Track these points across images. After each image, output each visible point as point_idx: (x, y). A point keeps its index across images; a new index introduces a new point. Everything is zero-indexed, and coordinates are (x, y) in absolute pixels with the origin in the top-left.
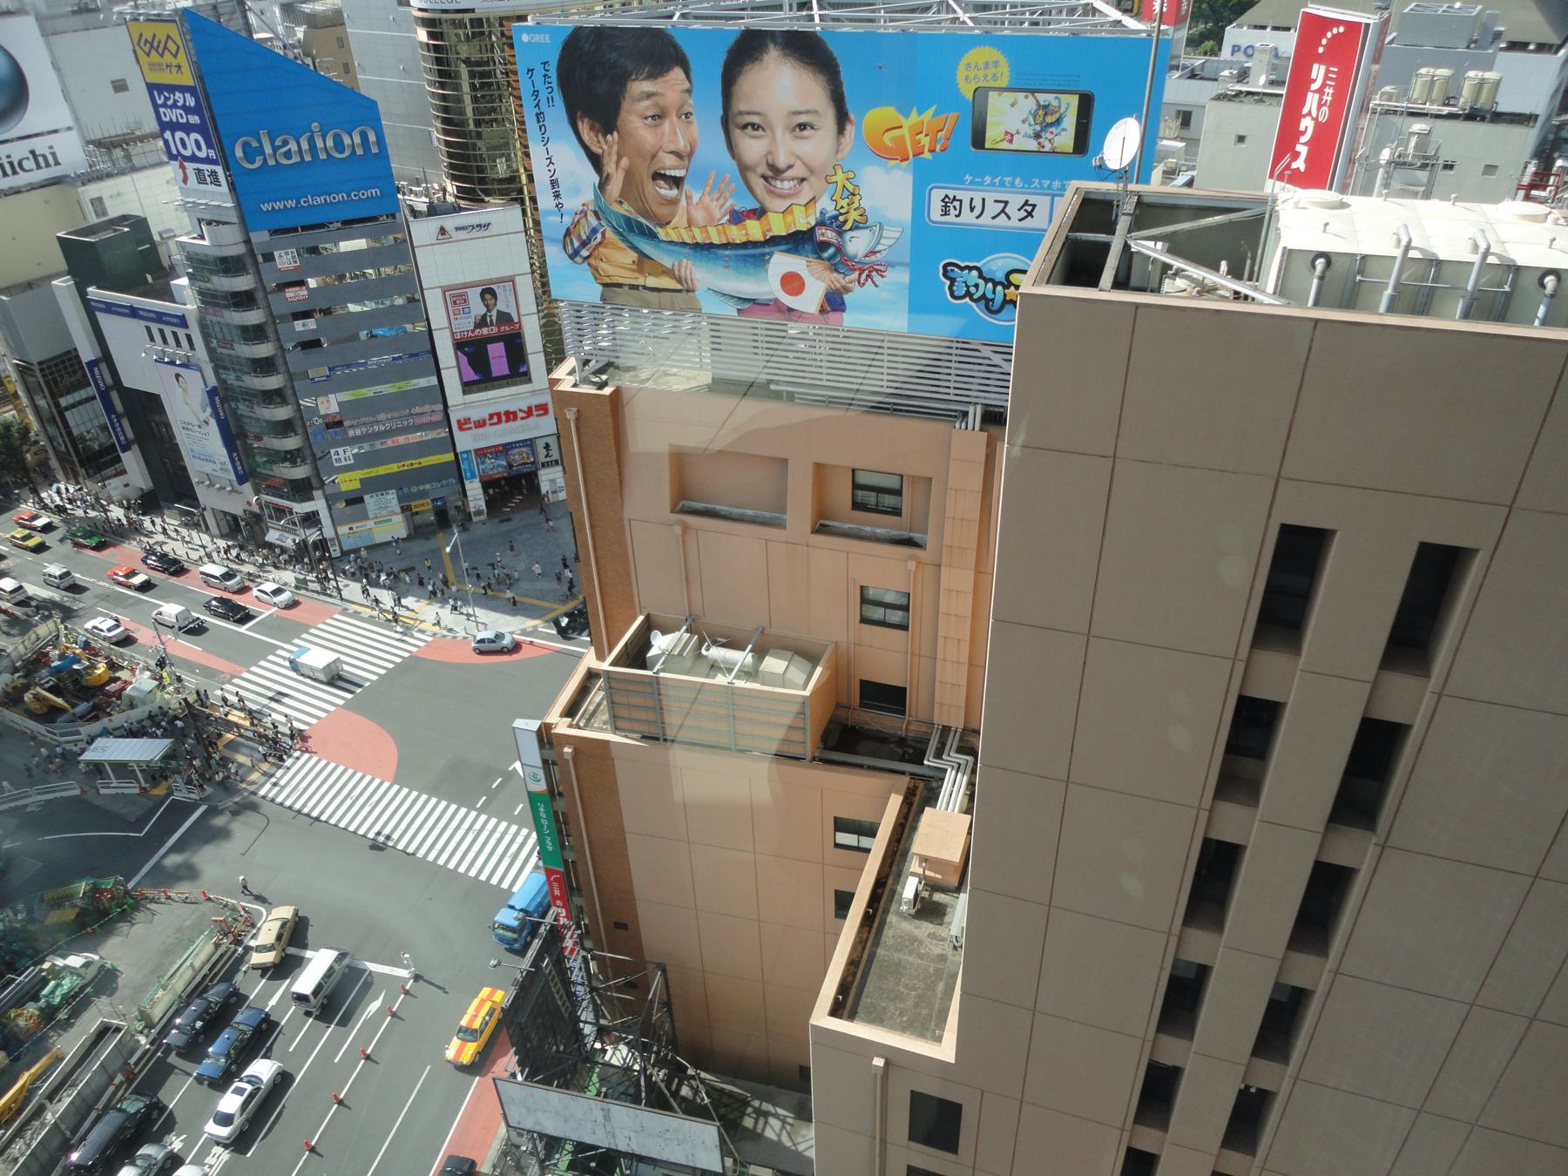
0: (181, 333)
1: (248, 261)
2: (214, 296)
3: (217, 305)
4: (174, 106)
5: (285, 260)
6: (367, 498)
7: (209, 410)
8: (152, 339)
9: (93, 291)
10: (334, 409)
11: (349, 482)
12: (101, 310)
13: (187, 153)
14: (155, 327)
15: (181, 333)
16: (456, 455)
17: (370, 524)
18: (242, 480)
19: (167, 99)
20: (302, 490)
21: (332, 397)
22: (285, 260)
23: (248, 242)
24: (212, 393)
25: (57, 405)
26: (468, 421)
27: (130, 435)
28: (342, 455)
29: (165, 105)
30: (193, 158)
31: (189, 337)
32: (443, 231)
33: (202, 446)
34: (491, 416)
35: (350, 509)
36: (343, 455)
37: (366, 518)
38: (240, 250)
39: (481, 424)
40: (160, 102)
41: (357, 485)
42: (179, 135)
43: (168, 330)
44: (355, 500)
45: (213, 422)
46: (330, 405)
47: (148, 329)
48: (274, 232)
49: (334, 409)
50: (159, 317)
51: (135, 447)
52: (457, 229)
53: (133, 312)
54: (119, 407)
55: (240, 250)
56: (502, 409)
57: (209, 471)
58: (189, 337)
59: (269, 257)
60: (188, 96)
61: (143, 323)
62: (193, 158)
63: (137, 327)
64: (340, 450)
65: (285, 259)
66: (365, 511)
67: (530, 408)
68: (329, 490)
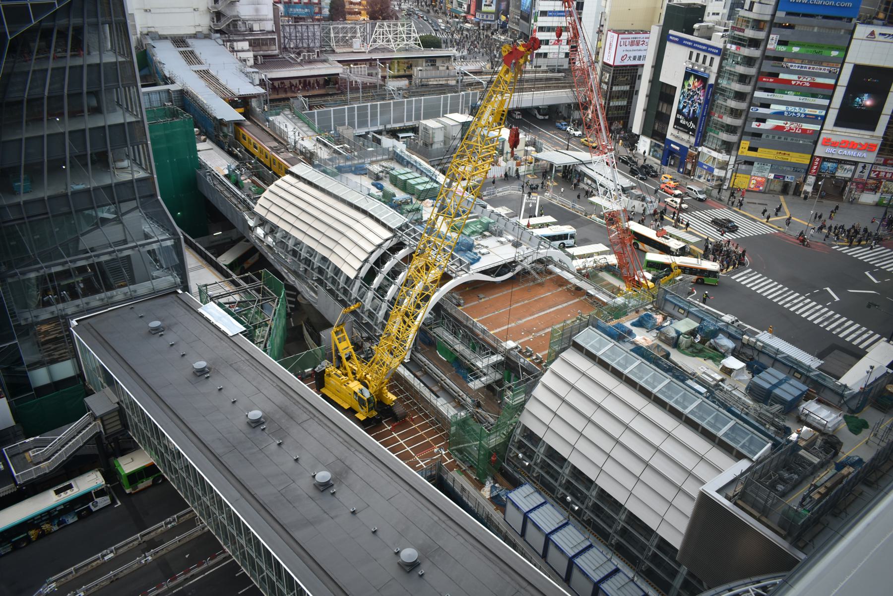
1: (768, 25)
2: (740, 39)
6: (756, 164)
8: (690, 58)
9: (671, 32)
14: (695, 52)
16: (813, 158)
23: (773, 15)
25: (611, 88)
26: (829, 140)
32: (872, 33)
34: (844, 142)
35: (744, 167)
38: (768, 18)
39: (834, 145)
47: (691, 53)
48: (788, 14)
52: (880, 34)
55: (768, 18)
56: (850, 139)
61: (689, 50)
67: (866, 144)
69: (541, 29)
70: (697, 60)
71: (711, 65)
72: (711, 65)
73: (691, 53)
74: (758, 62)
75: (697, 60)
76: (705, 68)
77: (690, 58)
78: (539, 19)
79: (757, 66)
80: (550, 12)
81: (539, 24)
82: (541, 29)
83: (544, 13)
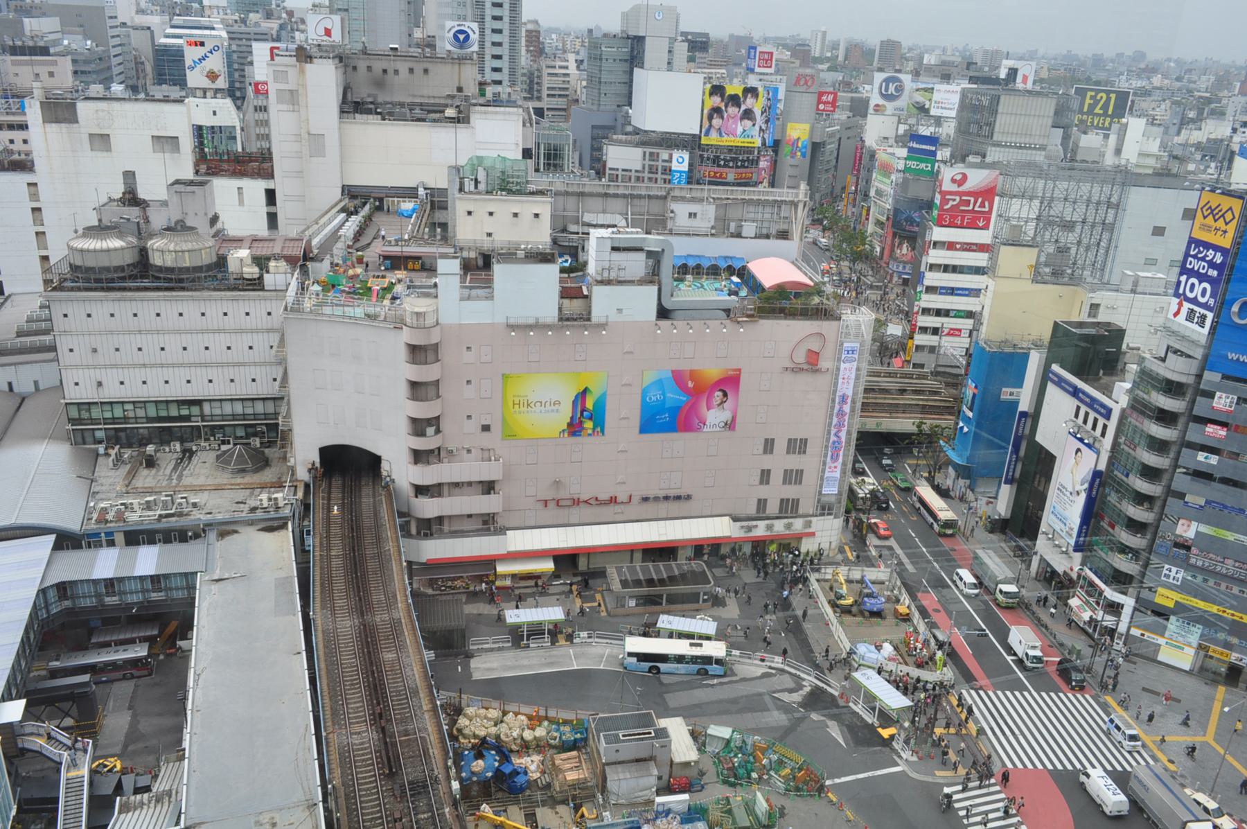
0: (1101, 421)
2: (1145, 406)
3: (1143, 413)
4: (1203, 259)
5: (1223, 402)
6: (1173, 618)
7: (1086, 486)
8: (1077, 416)
9: (1055, 368)
10: (1190, 534)
11: (1165, 597)
12: (1053, 381)
13: (1191, 296)
14: (1083, 409)
15: (1101, 421)
17: (1161, 641)
18: (1077, 548)
19: (1200, 252)
20: (1120, 580)
21: (1194, 525)
22: (1223, 402)
23: (1199, 377)
24: (1096, 474)
27: (1017, 475)
28: (1173, 574)
29: (1195, 257)
30: (1194, 301)
31: (1105, 427)
33: (1064, 508)
36: (1175, 574)
37: (1162, 635)
38: (1190, 380)
40: (1192, 253)
41: (1171, 605)
42: (1194, 280)
43: (1092, 415)
44: (1162, 613)
45: (1083, 496)
46: (1188, 530)
47: (1078, 408)
48: (1225, 377)
49: (1190, 534)
50: (1092, 403)
51: (1015, 486)
53: (1075, 392)
54: (1022, 453)
55: (1190, 380)
57: (1058, 529)
58: (1105, 427)
59: (1211, 395)
60: (1219, 254)
61: (1077, 402)
62: (1194, 301)
63: (1070, 403)
64: (1174, 569)
65: (1222, 401)
66: (1165, 627)
68: (1145, 594)
69: (926, 311)
70: (1085, 422)
71: (1103, 435)
72: (1103, 435)
73: (1078, 408)
74: (1174, 449)
75: (1085, 422)
76: (1095, 439)
77: (1077, 416)
78: (925, 297)
79: (1172, 455)
80: (942, 288)
81: (924, 305)
82: (926, 311)
83: (930, 290)
